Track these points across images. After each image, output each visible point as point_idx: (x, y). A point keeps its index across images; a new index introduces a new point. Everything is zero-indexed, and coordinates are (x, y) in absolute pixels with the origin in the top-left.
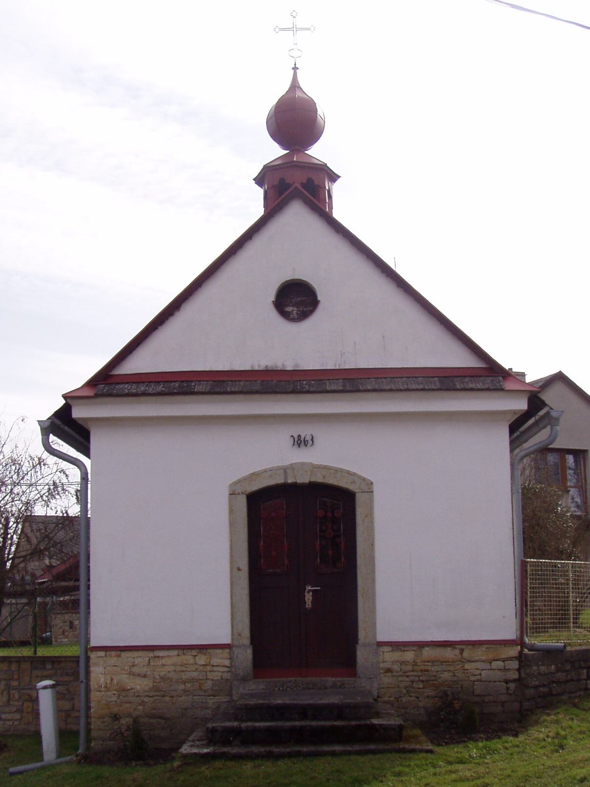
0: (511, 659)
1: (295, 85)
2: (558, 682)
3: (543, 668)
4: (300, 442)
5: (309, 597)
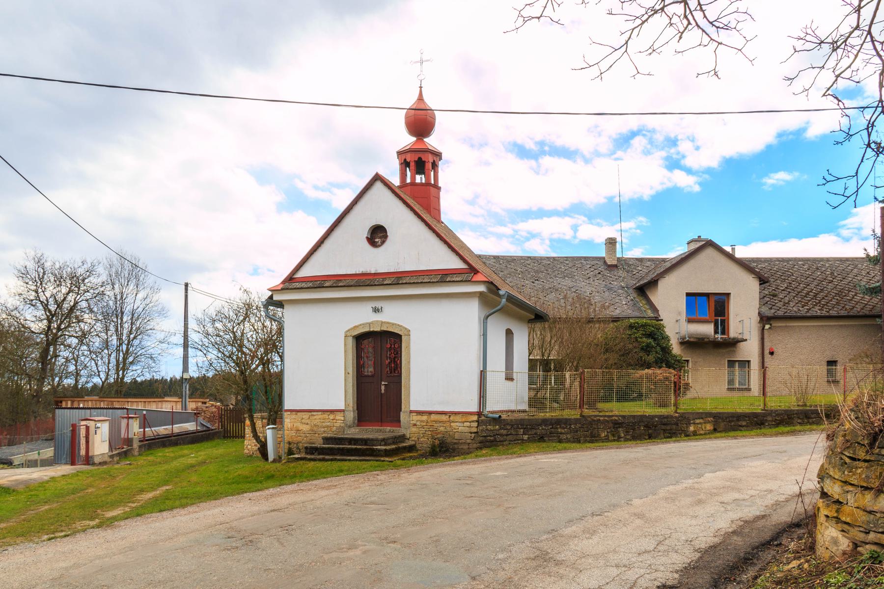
0: (473, 421)
1: (421, 98)
2: (502, 435)
3: (489, 427)
4: (376, 310)
5: (383, 388)
